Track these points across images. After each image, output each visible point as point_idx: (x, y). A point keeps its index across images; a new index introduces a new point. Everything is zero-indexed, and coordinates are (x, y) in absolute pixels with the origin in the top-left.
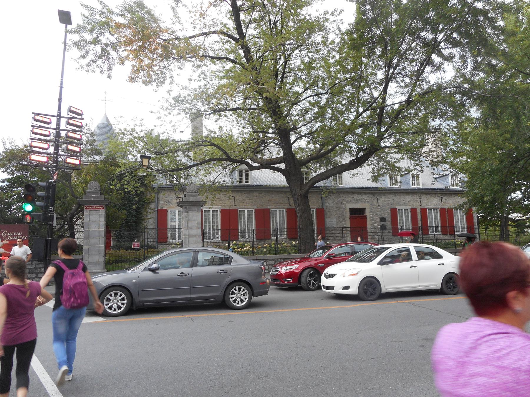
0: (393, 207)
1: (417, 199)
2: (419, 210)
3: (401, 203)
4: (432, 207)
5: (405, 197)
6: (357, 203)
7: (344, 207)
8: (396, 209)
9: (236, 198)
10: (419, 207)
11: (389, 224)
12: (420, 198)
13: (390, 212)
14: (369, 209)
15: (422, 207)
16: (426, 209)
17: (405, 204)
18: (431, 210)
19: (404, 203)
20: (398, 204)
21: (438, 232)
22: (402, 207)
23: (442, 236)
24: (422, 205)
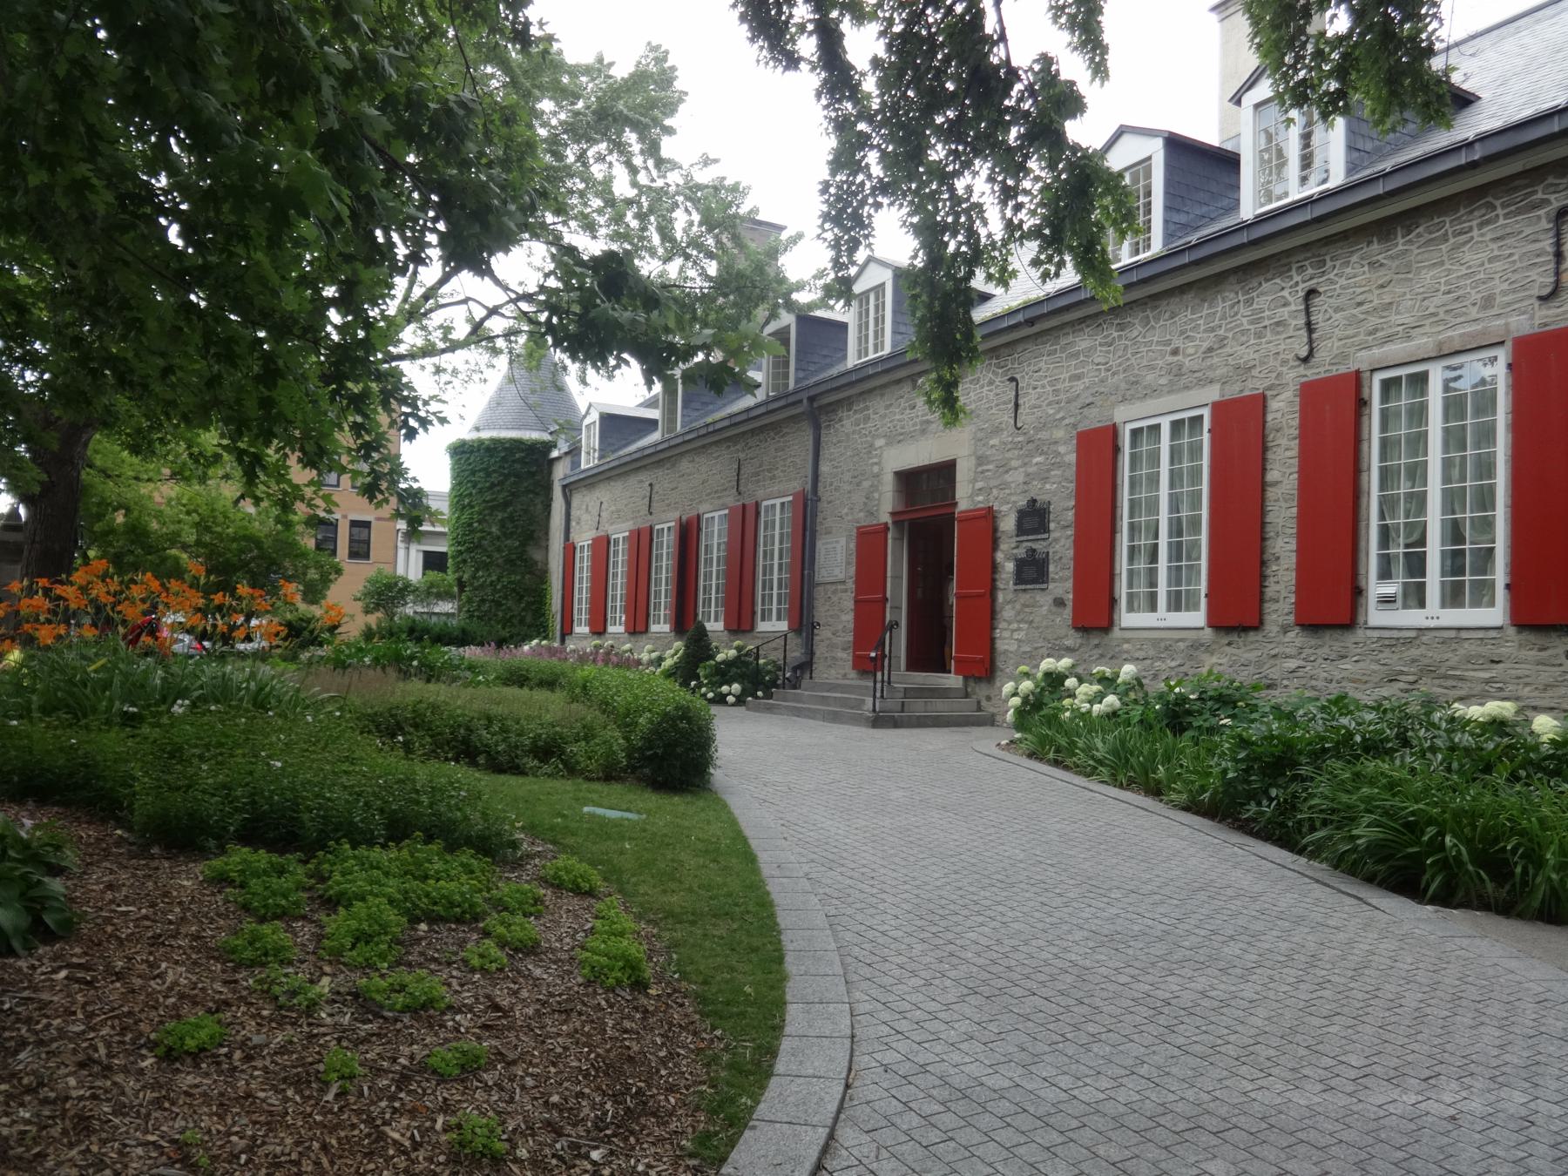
0: (1093, 420)
1: (1284, 313)
2: (1284, 412)
3: (1150, 378)
4: (1423, 342)
5: (1186, 316)
6: (923, 432)
7: (876, 469)
8: (1113, 431)
9: (656, 488)
10: (1294, 376)
11: (1060, 544)
12: (1311, 293)
13: (1072, 458)
14: (973, 460)
15: (1321, 369)
16: (1357, 380)
17: (1179, 379)
18: (1420, 381)
19: (1177, 372)
20: (1135, 390)
21: (1483, 593)
22: (1152, 405)
23: (1513, 645)
24: (1322, 355)
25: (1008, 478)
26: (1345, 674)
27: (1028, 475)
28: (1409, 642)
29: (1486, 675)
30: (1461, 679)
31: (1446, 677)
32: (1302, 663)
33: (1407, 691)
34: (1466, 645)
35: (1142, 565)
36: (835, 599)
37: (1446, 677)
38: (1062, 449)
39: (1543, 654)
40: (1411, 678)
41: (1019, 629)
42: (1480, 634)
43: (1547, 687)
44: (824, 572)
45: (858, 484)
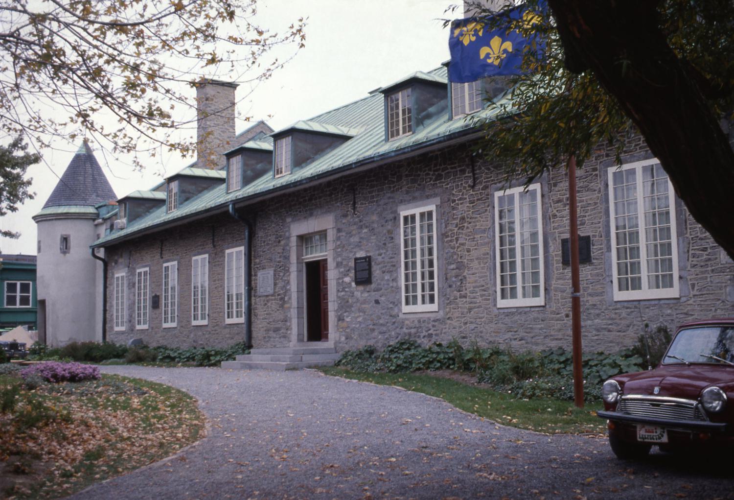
25: (352, 240)
26: (492, 330)
27: (361, 238)
28: (513, 314)
29: (539, 326)
30: (531, 328)
31: (527, 328)
32: (476, 325)
33: (515, 335)
34: (533, 313)
35: (427, 281)
36: (269, 304)
37: (527, 329)
38: (375, 225)
39: (558, 316)
40: (515, 329)
41: (360, 316)
42: (537, 309)
43: (560, 330)
44: (262, 290)
45: (279, 242)
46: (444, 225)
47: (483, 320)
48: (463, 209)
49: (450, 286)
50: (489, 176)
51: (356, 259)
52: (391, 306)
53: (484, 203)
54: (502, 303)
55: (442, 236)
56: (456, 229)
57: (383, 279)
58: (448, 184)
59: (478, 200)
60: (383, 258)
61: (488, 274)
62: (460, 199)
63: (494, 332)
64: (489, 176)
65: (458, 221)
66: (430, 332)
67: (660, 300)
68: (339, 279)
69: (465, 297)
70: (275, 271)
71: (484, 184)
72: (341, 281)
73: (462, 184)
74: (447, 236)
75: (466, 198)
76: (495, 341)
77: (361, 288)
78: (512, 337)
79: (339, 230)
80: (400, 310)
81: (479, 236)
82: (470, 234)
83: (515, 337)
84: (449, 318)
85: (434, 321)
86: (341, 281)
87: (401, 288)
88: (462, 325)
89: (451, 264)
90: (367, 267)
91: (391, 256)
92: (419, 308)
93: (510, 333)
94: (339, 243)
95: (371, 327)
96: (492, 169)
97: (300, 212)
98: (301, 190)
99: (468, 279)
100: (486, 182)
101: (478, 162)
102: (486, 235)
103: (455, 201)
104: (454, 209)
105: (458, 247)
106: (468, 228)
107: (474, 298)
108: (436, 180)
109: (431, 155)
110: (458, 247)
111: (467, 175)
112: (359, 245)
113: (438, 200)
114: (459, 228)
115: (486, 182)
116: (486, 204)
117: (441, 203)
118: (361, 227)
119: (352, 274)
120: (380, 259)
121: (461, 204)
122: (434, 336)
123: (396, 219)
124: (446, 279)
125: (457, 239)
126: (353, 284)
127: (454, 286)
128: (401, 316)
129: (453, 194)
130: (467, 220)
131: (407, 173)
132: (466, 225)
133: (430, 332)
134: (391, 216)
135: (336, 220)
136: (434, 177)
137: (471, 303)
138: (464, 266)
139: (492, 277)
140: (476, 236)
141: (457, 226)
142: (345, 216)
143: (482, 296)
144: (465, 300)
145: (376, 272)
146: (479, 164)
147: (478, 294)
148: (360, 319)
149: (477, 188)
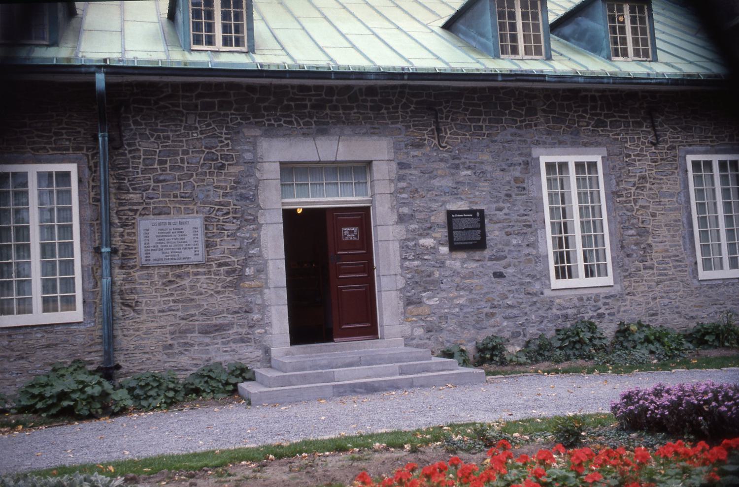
14: (394, 165)
26: (692, 303)
27: (458, 183)
28: (718, 286)
33: (720, 308)
38: (489, 168)
40: (722, 302)
41: (462, 296)
46: (614, 181)
47: (678, 294)
48: (642, 166)
49: (628, 256)
50: (676, 136)
51: (450, 213)
52: (528, 280)
53: (672, 164)
54: (703, 275)
55: (612, 195)
56: (634, 188)
57: (507, 244)
58: (618, 134)
59: (662, 160)
60: (506, 214)
61: (681, 243)
62: (638, 155)
63: (695, 306)
64: (676, 136)
65: (636, 180)
66: (600, 311)
67: (723, 279)
68: (407, 240)
69: (652, 268)
70: (206, 219)
71: (669, 144)
72: (412, 244)
73: (639, 138)
74: (619, 196)
75: (646, 156)
76: (696, 316)
77: (461, 255)
78: (718, 310)
79: (402, 165)
80: (549, 286)
81: (667, 200)
82: (655, 196)
83: (722, 310)
84: (628, 294)
85: (606, 297)
86: (412, 244)
87: (547, 256)
88: (650, 300)
89: (628, 229)
90: (479, 226)
91: (522, 212)
92: (580, 281)
93: (715, 306)
94: (402, 184)
95: (487, 310)
96: (680, 130)
97: (290, 123)
98: (293, 87)
99: (655, 248)
100: (673, 142)
101: (659, 118)
102: (675, 199)
103: (630, 155)
104: (628, 165)
105: (638, 210)
106: (650, 189)
107: (665, 269)
108: (597, 126)
109: (585, 93)
110: (638, 210)
111: (644, 129)
112: (454, 193)
113: (604, 151)
114: (637, 188)
115: (673, 142)
116: (674, 166)
117: (609, 155)
118: (457, 167)
119: (442, 233)
120: (500, 215)
121: (639, 160)
122: (607, 316)
123: (530, 165)
124: (622, 247)
125: (635, 201)
126: (444, 250)
127: (635, 255)
128: (547, 293)
129: (626, 147)
130: (649, 180)
131: (545, 107)
132: (648, 185)
133: (600, 311)
134: (520, 159)
135: (397, 149)
136: (593, 123)
137: (660, 275)
138: (648, 232)
139: (688, 246)
140: (662, 200)
141: (634, 185)
142: (418, 146)
143: (675, 267)
144: (651, 272)
145: (494, 233)
146: (660, 120)
147: (671, 265)
148: (461, 301)
149: (660, 146)
